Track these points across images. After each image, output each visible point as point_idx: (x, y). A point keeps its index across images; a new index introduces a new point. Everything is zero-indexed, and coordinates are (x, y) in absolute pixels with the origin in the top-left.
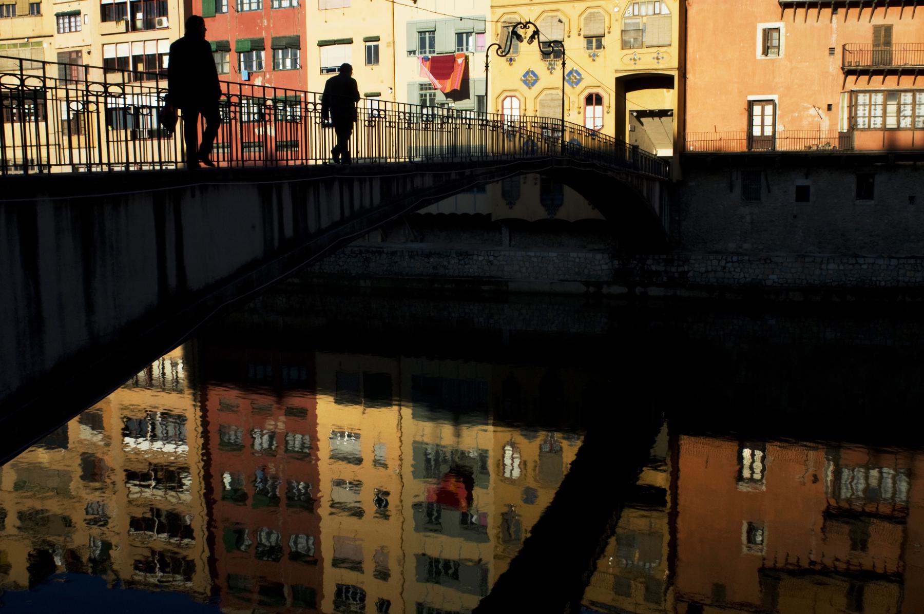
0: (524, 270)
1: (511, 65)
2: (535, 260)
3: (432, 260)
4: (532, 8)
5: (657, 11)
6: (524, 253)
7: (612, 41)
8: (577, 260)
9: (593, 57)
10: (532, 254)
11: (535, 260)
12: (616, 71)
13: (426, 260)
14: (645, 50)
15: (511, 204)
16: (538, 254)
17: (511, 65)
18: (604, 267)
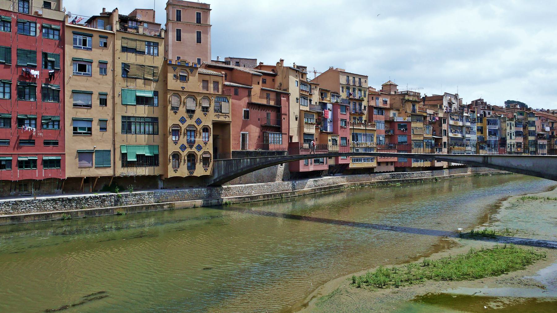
0: (176, 198)
1: (175, 114)
2: (180, 193)
3: (136, 197)
4: (183, 92)
5: (225, 101)
6: (176, 191)
7: (211, 109)
8: (196, 192)
9: (205, 115)
10: (179, 191)
11: (180, 193)
12: (213, 120)
13: (134, 197)
14: (220, 114)
15: (176, 171)
16: (181, 191)
17: (175, 114)
18: (205, 193)
